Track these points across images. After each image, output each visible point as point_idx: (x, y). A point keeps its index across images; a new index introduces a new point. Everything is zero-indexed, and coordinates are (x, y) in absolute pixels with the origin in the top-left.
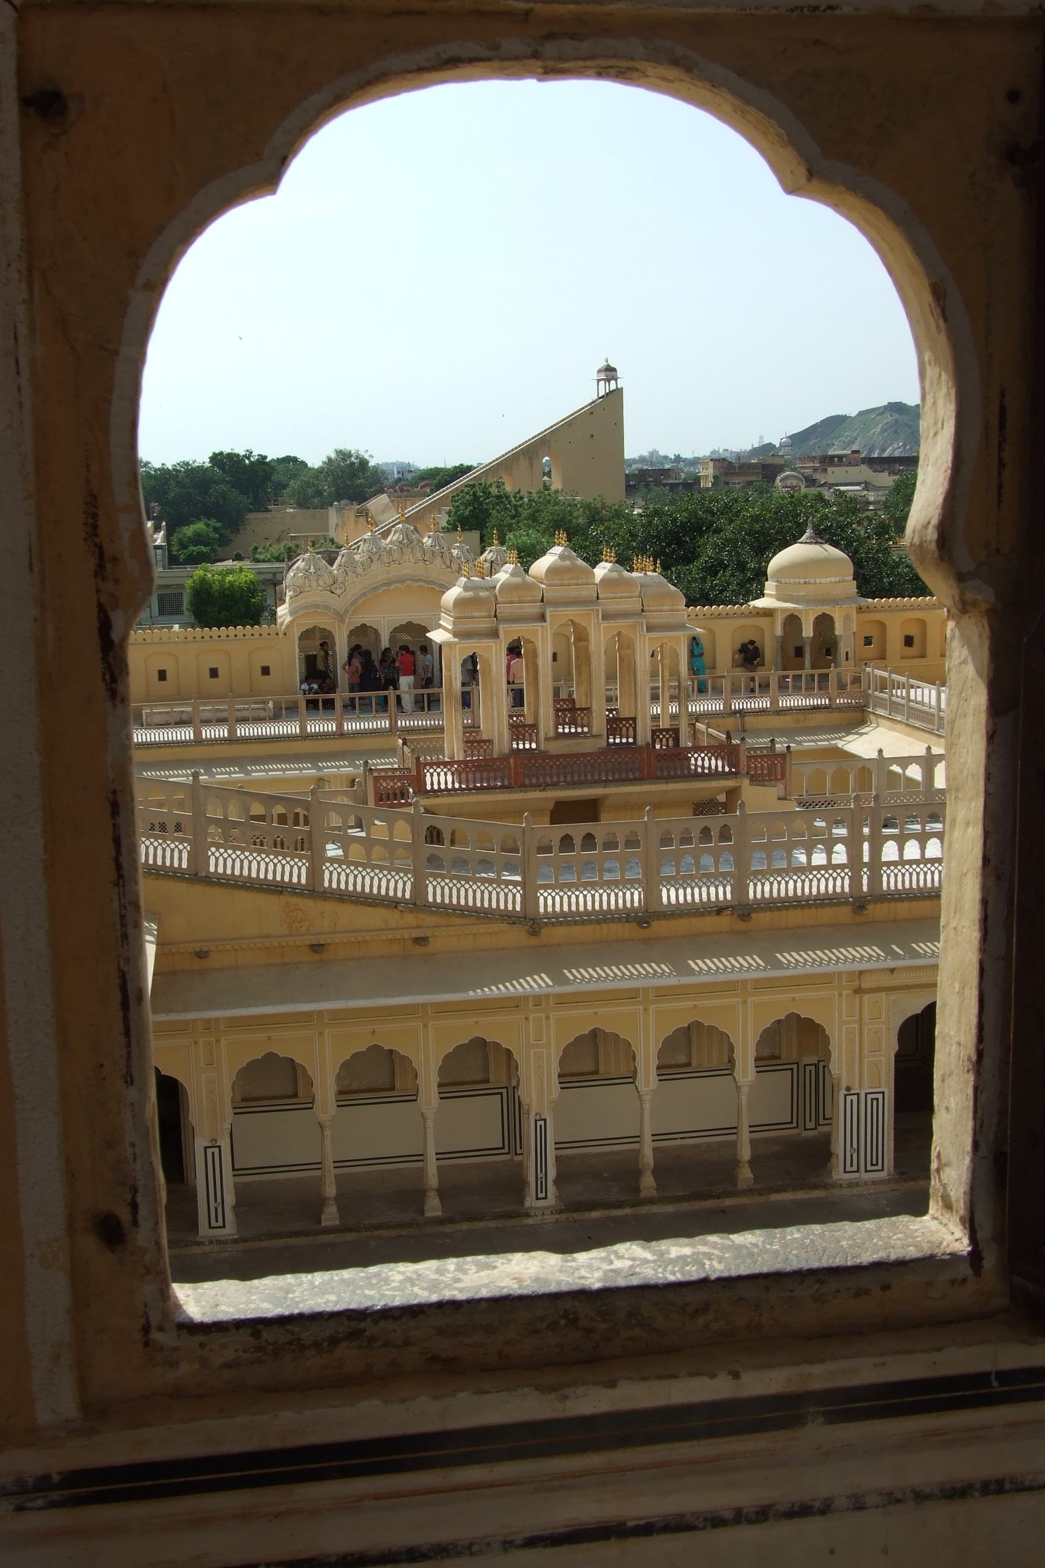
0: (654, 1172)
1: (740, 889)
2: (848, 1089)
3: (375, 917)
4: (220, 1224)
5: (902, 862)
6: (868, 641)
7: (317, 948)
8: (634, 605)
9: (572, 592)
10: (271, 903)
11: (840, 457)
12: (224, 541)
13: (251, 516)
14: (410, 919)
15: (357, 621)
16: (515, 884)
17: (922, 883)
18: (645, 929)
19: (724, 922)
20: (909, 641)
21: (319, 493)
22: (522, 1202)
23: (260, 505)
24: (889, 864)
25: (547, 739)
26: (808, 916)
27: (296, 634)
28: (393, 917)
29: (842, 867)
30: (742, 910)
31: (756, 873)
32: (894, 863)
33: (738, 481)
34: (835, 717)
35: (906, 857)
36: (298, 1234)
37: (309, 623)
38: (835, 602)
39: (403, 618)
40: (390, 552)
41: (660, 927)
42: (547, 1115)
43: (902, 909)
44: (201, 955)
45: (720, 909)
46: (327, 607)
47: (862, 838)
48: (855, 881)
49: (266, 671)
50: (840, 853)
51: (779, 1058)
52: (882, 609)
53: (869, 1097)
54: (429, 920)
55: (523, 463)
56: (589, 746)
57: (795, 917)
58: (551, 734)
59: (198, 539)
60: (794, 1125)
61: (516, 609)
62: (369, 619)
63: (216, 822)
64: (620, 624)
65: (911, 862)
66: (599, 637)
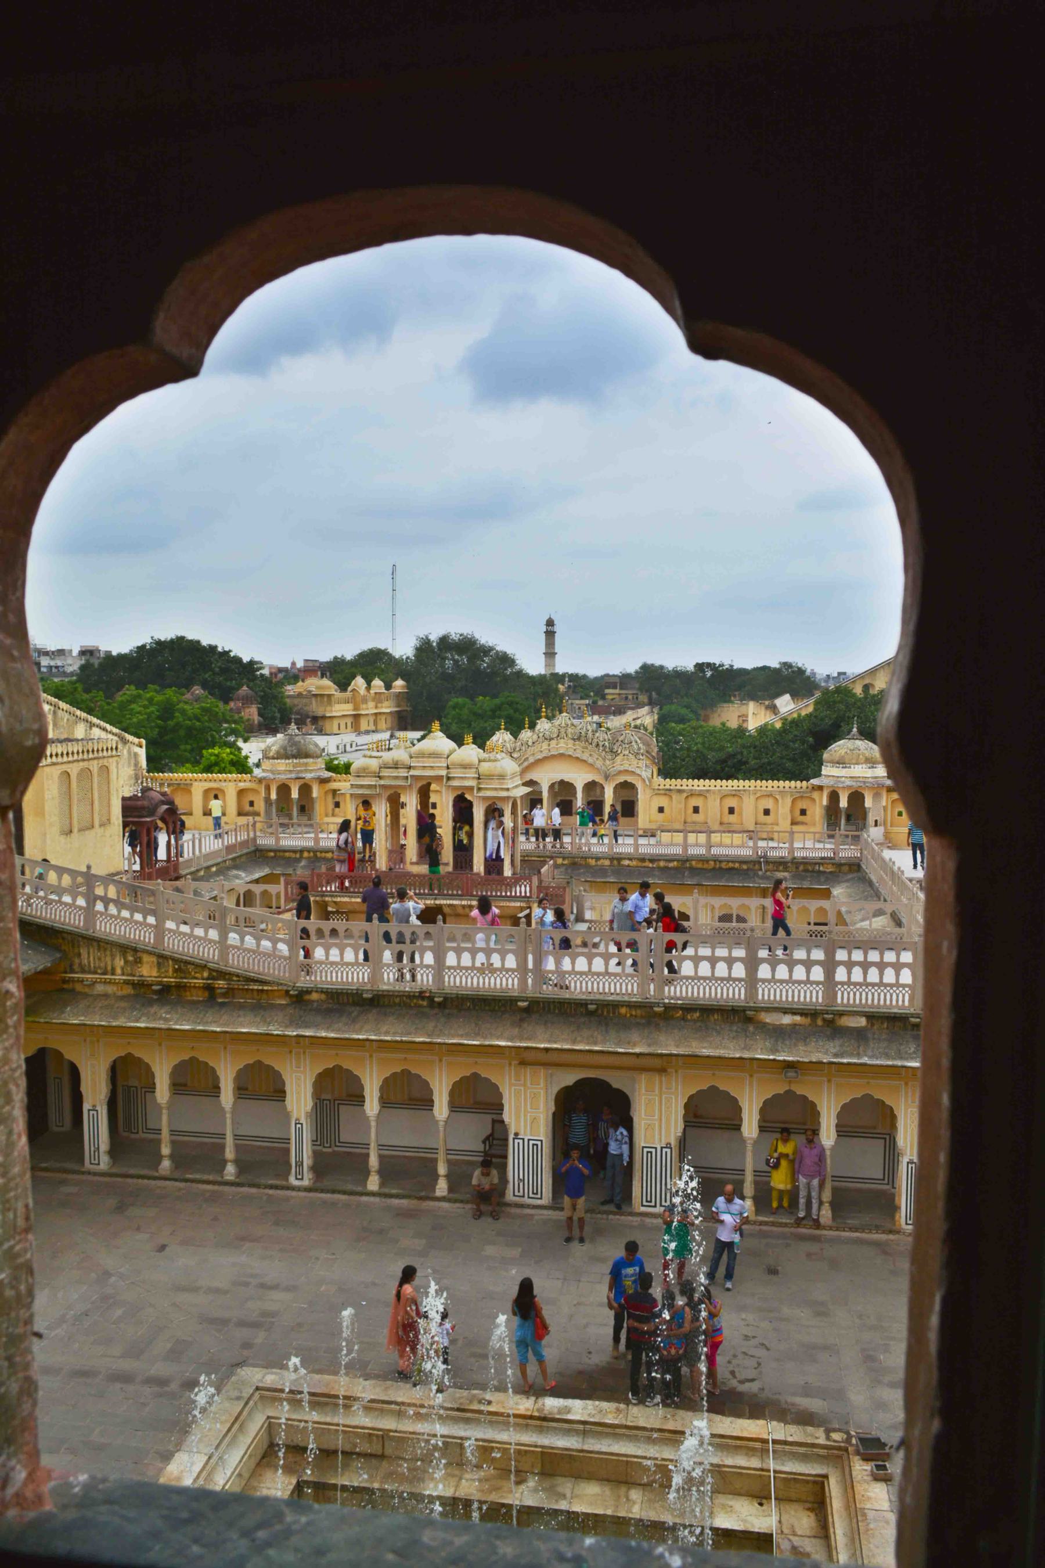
0: (380, 1172)
2: (516, 1134)
4: (521, 1194)
17: (731, 996)
22: (287, 1180)
25: (412, 863)
35: (700, 974)
36: (397, 1196)
39: (558, 777)
42: (303, 1121)
48: (523, 981)
51: (246, 1089)
53: (531, 1142)
58: (414, 860)
60: (886, 1181)
65: (855, 984)
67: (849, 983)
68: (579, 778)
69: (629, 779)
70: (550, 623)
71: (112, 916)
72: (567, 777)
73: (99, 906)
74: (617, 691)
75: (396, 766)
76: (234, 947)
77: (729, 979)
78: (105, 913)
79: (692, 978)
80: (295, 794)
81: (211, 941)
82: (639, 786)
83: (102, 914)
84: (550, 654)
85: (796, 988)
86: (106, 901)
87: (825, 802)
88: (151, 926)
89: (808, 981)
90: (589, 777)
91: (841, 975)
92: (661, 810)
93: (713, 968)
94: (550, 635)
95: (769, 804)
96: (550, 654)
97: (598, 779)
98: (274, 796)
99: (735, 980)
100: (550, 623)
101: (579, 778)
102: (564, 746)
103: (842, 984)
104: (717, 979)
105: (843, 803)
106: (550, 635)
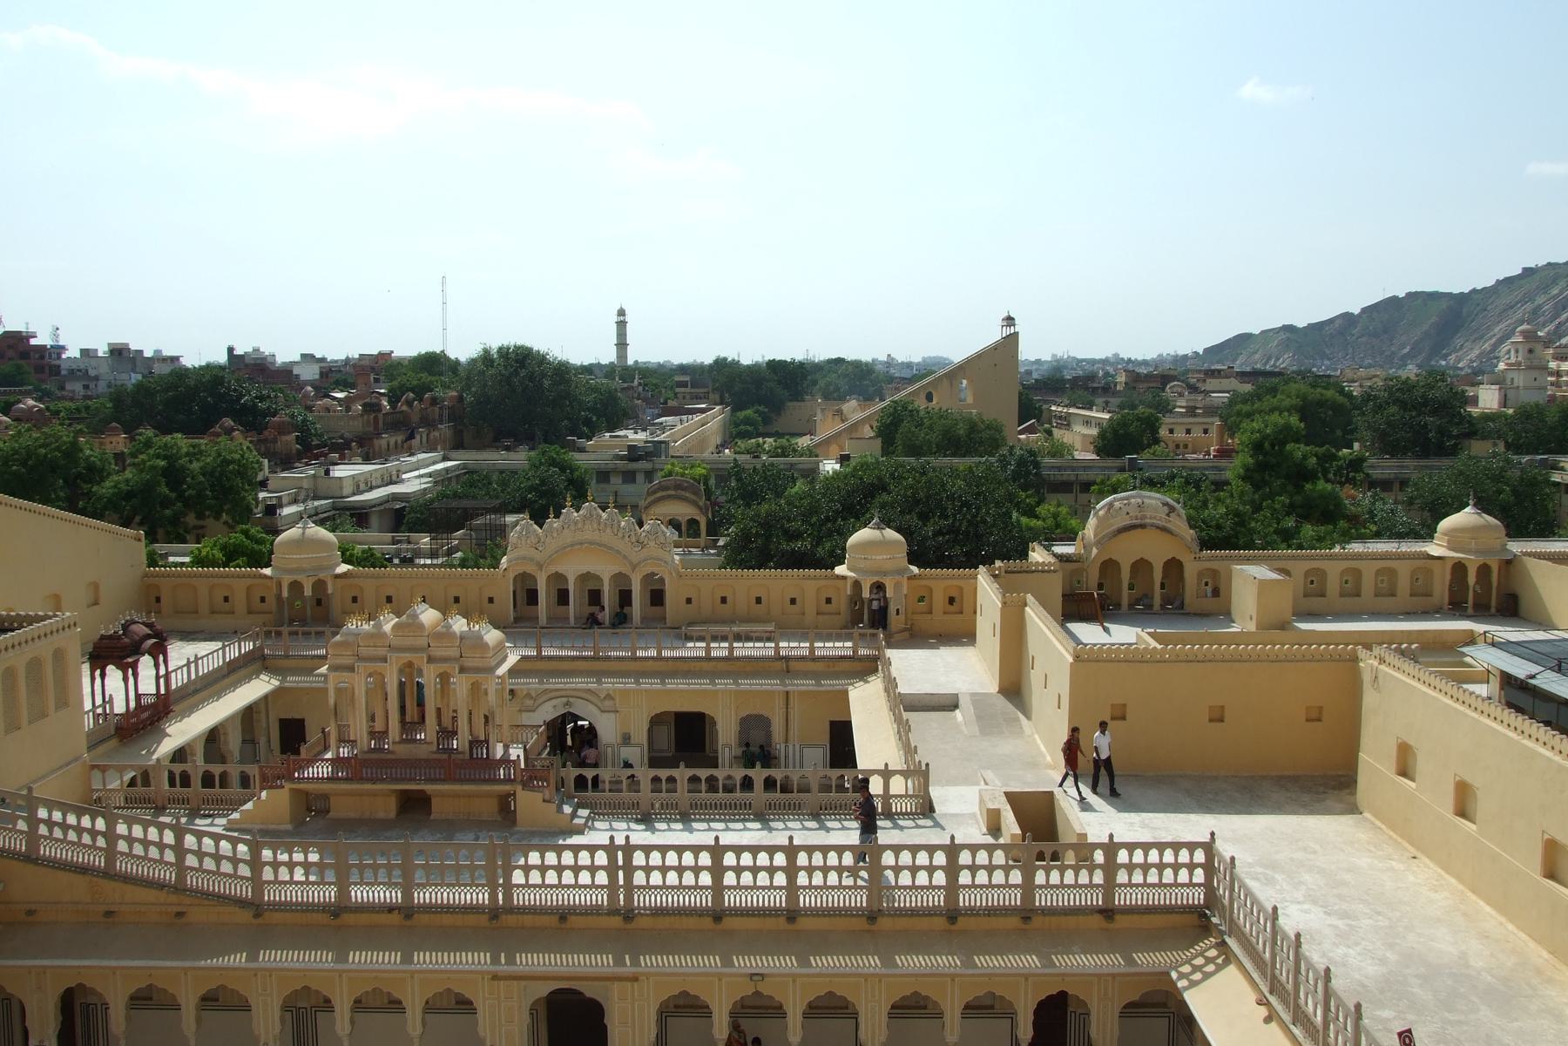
1: (407, 894)
3: (150, 895)
5: (527, 885)
6: (921, 599)
7: (109, 914)
8: (454, 652)
9: (408, 642)
10: (80, 881)
11: (1219, 371)
12: (767, 420)
13: (790, 404)
14: (173, 898)
15: (552, 569)
16: (247, 879)
18: (337, 923)
19: (395, 918)
20: (951, 600)
21: (837, 389)
23: (797, 396)
26: (458, 920)
27: (512, 576)
28: (162, 896)
30: (407, 911)
31: (419, 885)
33: (1142, 386)
34: (858, 666)
37: (520, 570)
38: (885, 574)
39: (584, 569)
40: (576, 523)
41: (348, 918)
43: (528, 920)
44: (30, 913)
45: (390, 909)
46: (532, 560)
49: (491, 600)
52: (931, 578)
54: (188, 901)
55: (946, 382)
56: (422, 752)
57: (447, 919)
59: (747, 421)
61: (371, 652)
62: (561, 569)
64: (443, 667)
66: (429, 678)
67: (810, 887)
68: (605, 570)
70: (621, 313)
71: (57, 840)
72: (592, 568)
73: (43, 830)
74: (688, 390)
76: (192, 869)
77: (696, 887)
78: (50, 837)
79: (661, 888)
80: (308, 592)
81: (167, 863)
84: (622, 345)
85: (760, 893)
88: (101, 849)
89: (771, 887)
90: (616, 569)
91: (802, 879)
92: (689, 601)
93: (680, 877)
94: (622, 325)
96: (622, 345)
97: (625, 570)
98: (285, 594)
99: (702, 888)
100: (621, 313)
103: (804, 888)
104: (685, 888)
106: (622, 325)
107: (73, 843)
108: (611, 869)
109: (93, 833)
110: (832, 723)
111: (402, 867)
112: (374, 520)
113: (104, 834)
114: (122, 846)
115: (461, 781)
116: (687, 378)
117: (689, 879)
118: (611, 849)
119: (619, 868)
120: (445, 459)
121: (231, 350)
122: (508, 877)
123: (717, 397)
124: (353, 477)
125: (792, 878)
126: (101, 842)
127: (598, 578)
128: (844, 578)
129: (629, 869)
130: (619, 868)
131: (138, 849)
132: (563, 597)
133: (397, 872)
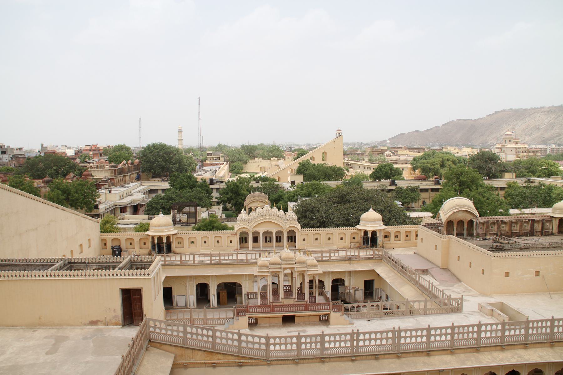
16: (264, 350)
24: (361, 346)
29: (349, 347)
32: (362, 346)
47: (354, 340)
48: (352, 350)
50: (348, 344)
58: (283, 297)
62: (257, 229)
63: (189, 333)
68: (274, 230)
69: (293, 229)
74: (212, 156)
75: (276, 264)
76: (244, 347)
80: (165, 241)
82: (296, 231)
83: (190, 339)
84: (180, 141)
86: (192, 334)
87: (363, 235)
88: (210, 342)
90: (278, 229)
95: (342, 236)
96: (180, 141)
97: (281, 229)
98: (156, 241)
99: (423, 342)
101: (274, 230)
102: (267, 218)
105: (370, 235)
107: (200, 340)
108: (393, 338)
109: (208, 336)
110: (366, 281)
111: (320, 342)
112: (128, 210)
113: (212, 337)
114: (218, 340)
115: (311, 310)
116: (211, 152)
117: (419, 340)
118: (393, 331)
119: (396, 337)
120: (141, 185)
121: (42, 145)
122: (358, 343)
123: (222, 159)
124: (119, 193)
125: (452, 337)
126: (210, 339)
127: (271, 233)
128: (360, 230)
129: (399, 338)
130: (396, 337)
131: (224, 341)
132: (256, 240)
133: (294, 345)
